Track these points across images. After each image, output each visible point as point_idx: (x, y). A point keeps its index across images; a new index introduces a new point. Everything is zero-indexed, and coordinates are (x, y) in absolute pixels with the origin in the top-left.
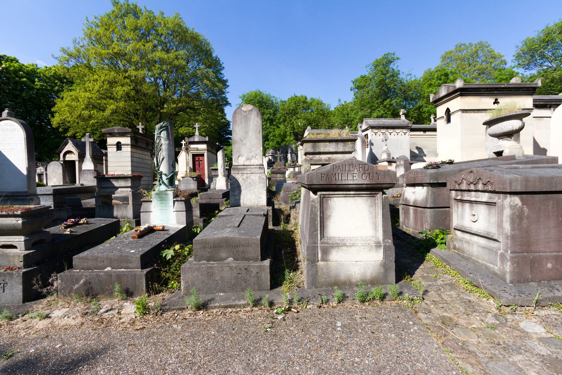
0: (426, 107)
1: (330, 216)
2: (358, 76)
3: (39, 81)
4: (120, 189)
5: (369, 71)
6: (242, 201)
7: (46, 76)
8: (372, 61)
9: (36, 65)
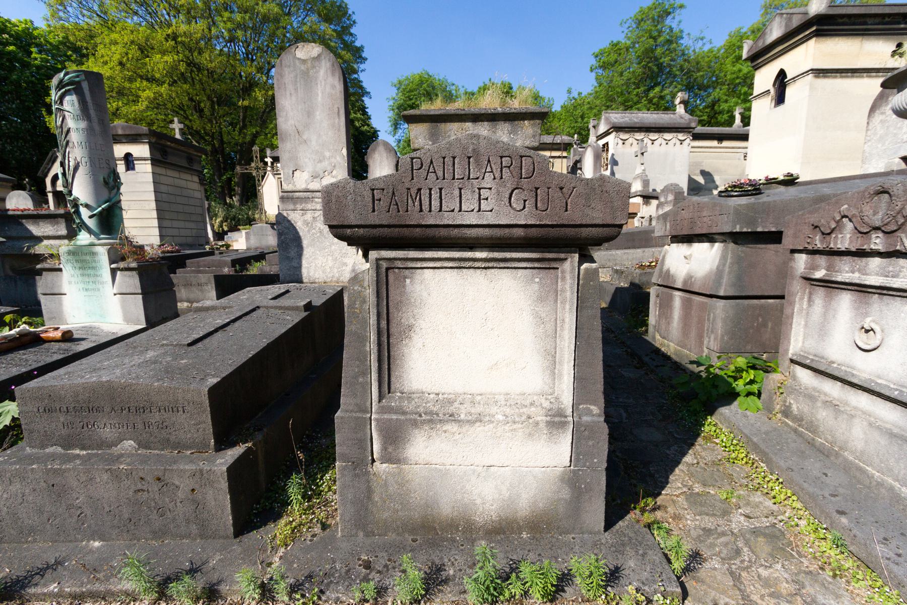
0: (726, 101)
1: (410, 327)
2: (605, 44)
3: (40, 52)
4: (46, 242)
5: (626, 31)
6: (304, 272)
7: (51, 44)
8: (633, 12)
9: (32, 22)
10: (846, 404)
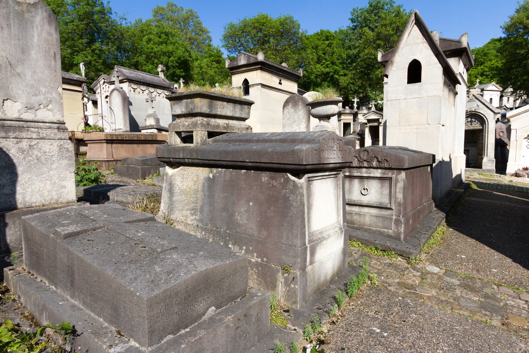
6: (19, 198)
10: (361, 212)
